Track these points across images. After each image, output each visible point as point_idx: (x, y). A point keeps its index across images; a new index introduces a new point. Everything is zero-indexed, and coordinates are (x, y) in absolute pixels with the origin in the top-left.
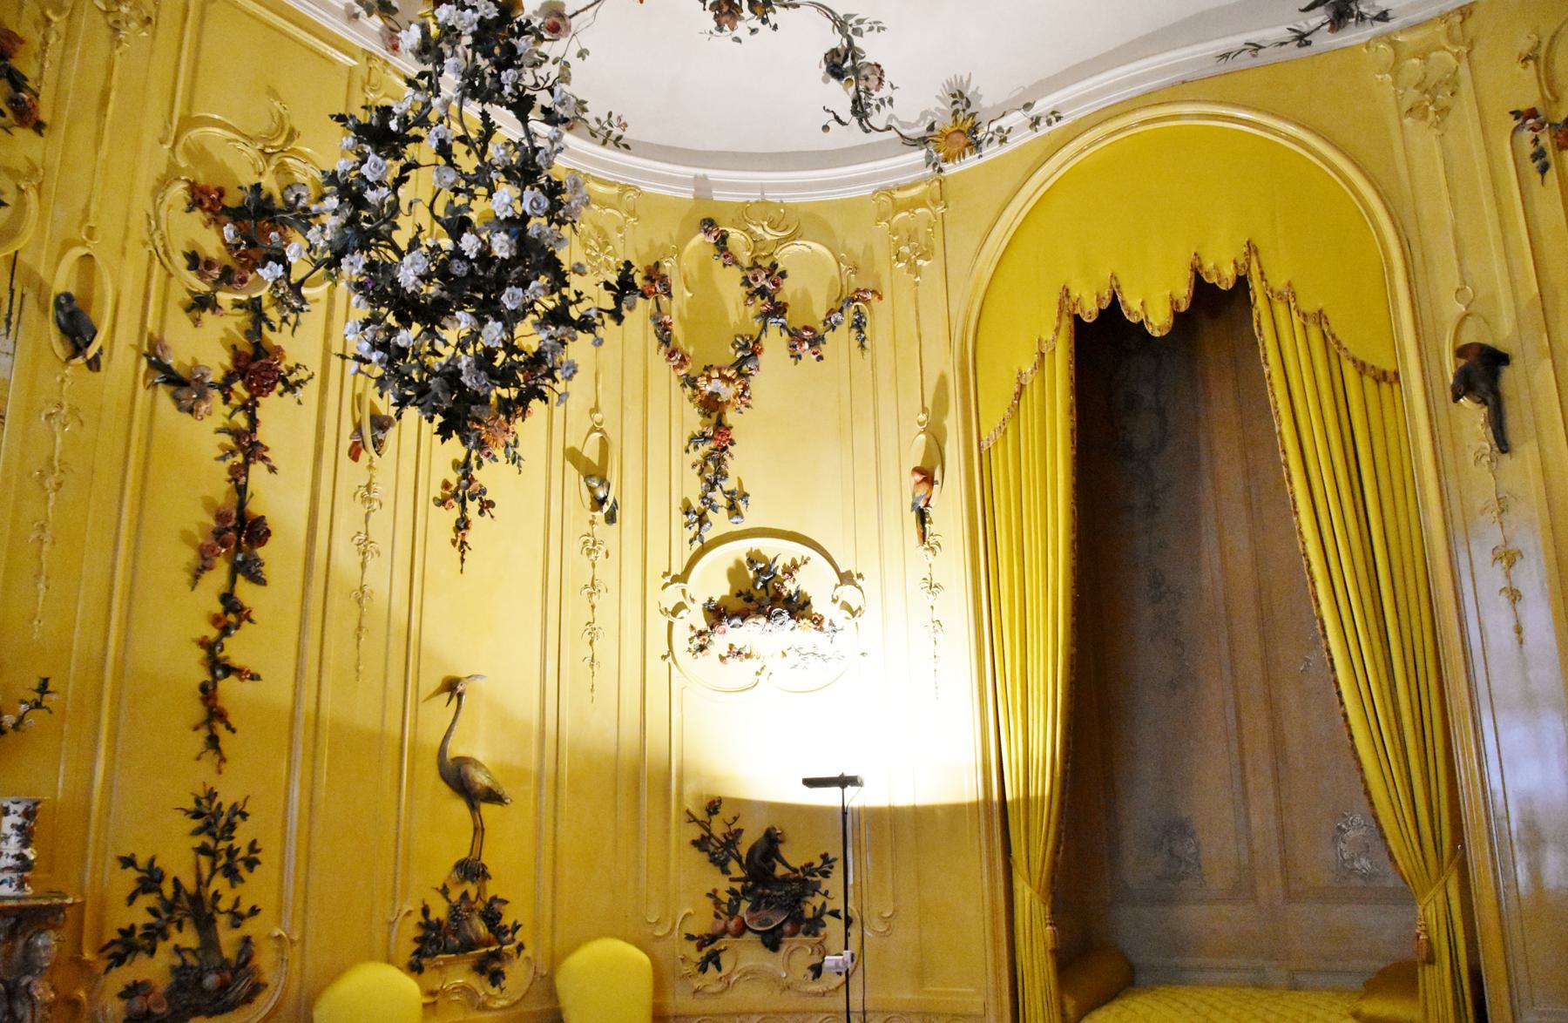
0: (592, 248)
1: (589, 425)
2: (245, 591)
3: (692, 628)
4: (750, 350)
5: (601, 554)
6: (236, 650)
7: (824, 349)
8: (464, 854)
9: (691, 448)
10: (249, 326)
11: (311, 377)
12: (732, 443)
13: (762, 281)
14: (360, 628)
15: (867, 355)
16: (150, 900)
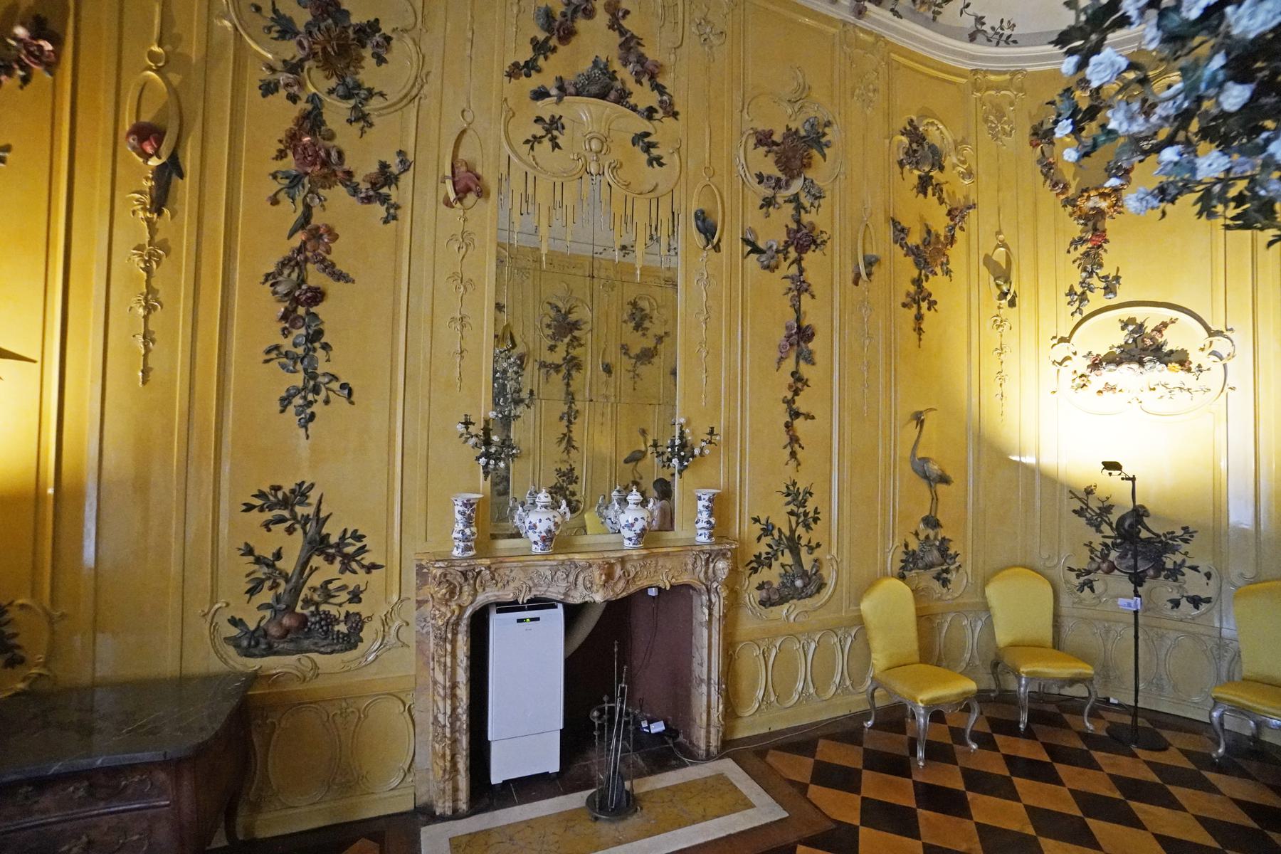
1: (997, 242)
2: (805, 369)
6: (801, 404)
8: (927, 513)
12: (1106, 241)
16: (768, 540)
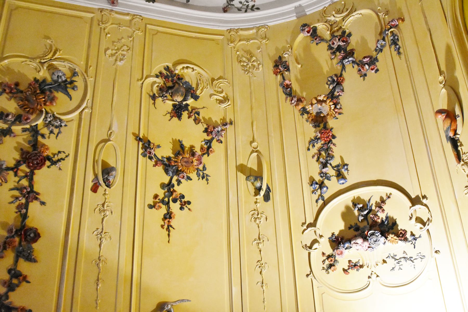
0: (244, 62)
3: (323, 254)
4: (337, 81)
5: (263, 220)
7: (379, 65)
9: (311, 147)
10: (31, 138)
11: (67, 156)
12: (334, 137)
13: (337, 43)
14: (98, 280)
15: (402, 56)
